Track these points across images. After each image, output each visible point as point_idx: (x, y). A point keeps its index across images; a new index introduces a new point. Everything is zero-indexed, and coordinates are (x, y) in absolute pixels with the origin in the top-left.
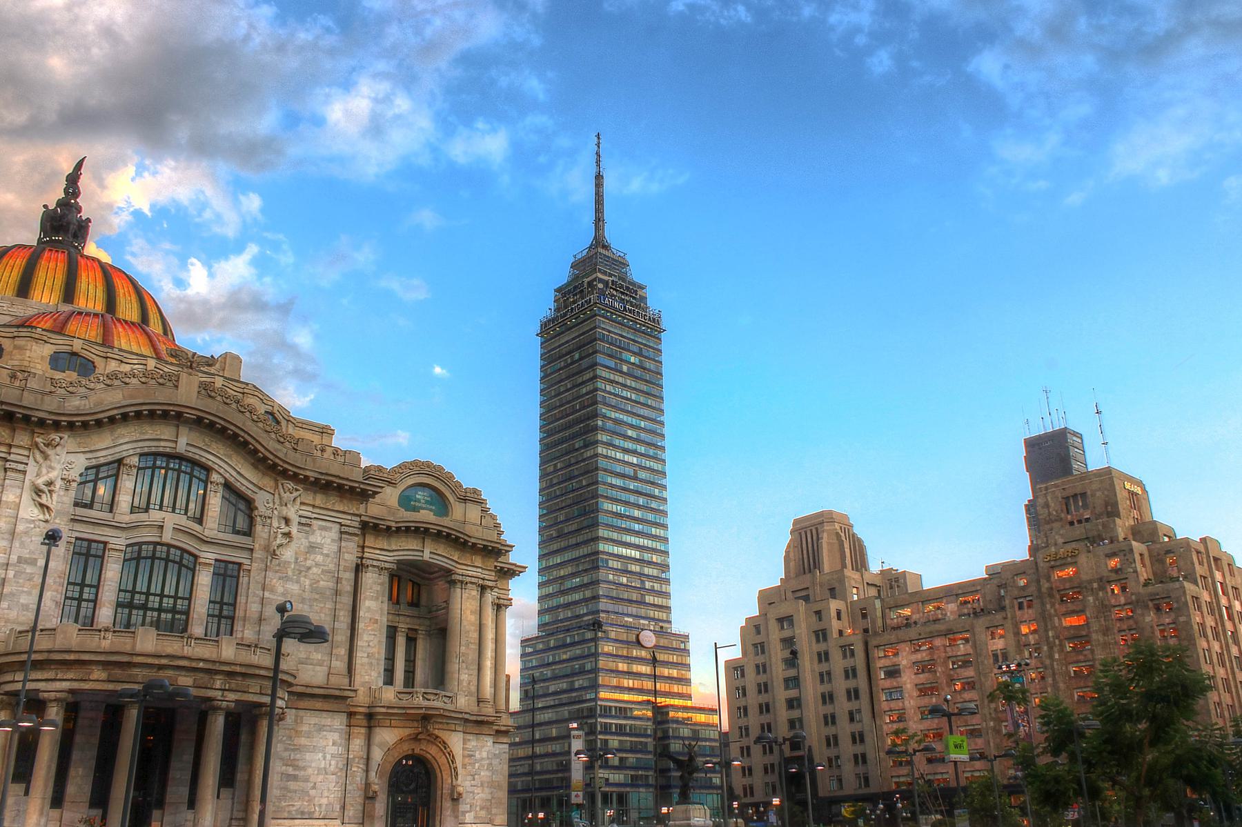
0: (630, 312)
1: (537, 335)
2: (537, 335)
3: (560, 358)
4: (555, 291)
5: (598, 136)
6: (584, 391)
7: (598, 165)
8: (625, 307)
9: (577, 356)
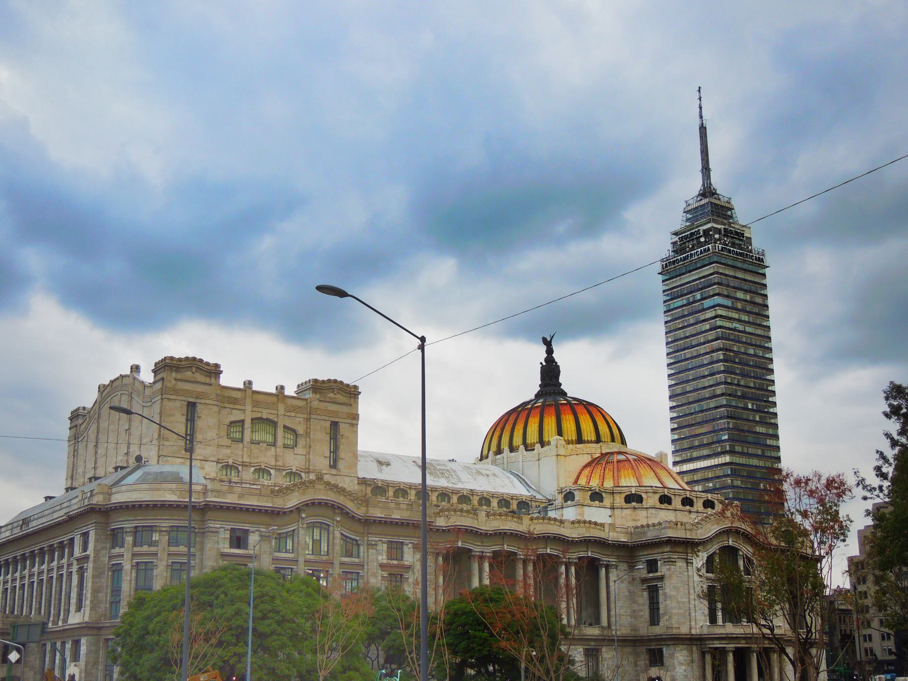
2: (659, 274)
3: (682, 296)
7: (701, 117)
9: (698, 297)
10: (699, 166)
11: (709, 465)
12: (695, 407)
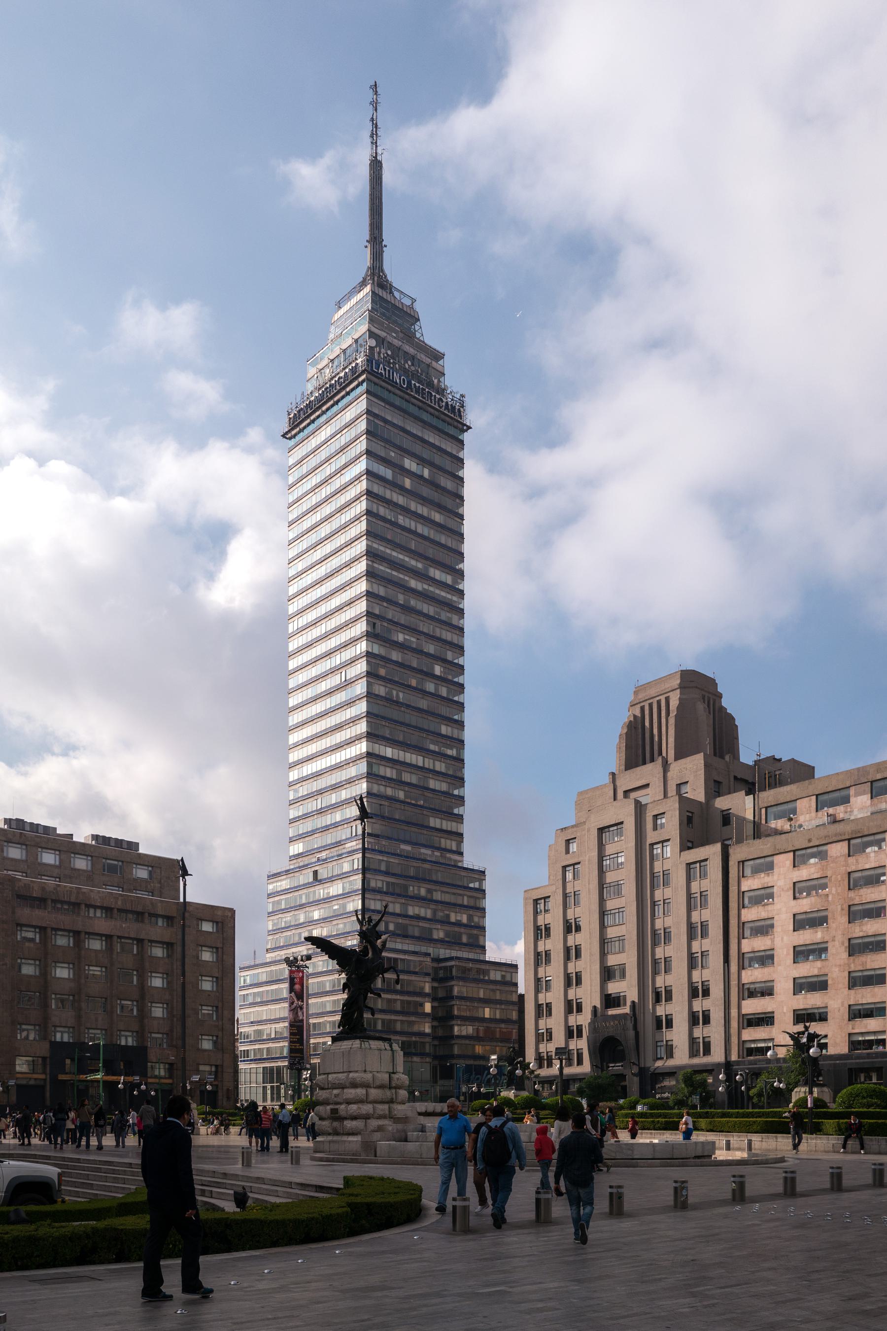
0: (417, 392)
5: (374, 88)
8: (409, 383)
10: (365, 233)
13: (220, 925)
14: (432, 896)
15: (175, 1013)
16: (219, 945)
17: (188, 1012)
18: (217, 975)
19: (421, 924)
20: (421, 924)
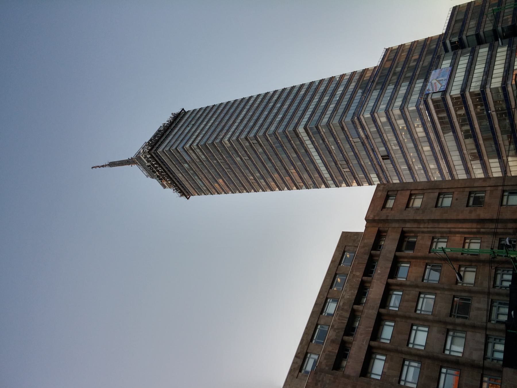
1: (188, 199)
2: (188, 199)
4: (165, 187)
6: (203, 157)
9: (186, 166)
11: (314, 150)
12: (269, 165)
13: (390, 193)
14: (398, 72)
15: (475, 230)
16: (408, 193)
17: (473, 216)
18: (437, 194)
19: (418, 73)
20: (418, 73)
